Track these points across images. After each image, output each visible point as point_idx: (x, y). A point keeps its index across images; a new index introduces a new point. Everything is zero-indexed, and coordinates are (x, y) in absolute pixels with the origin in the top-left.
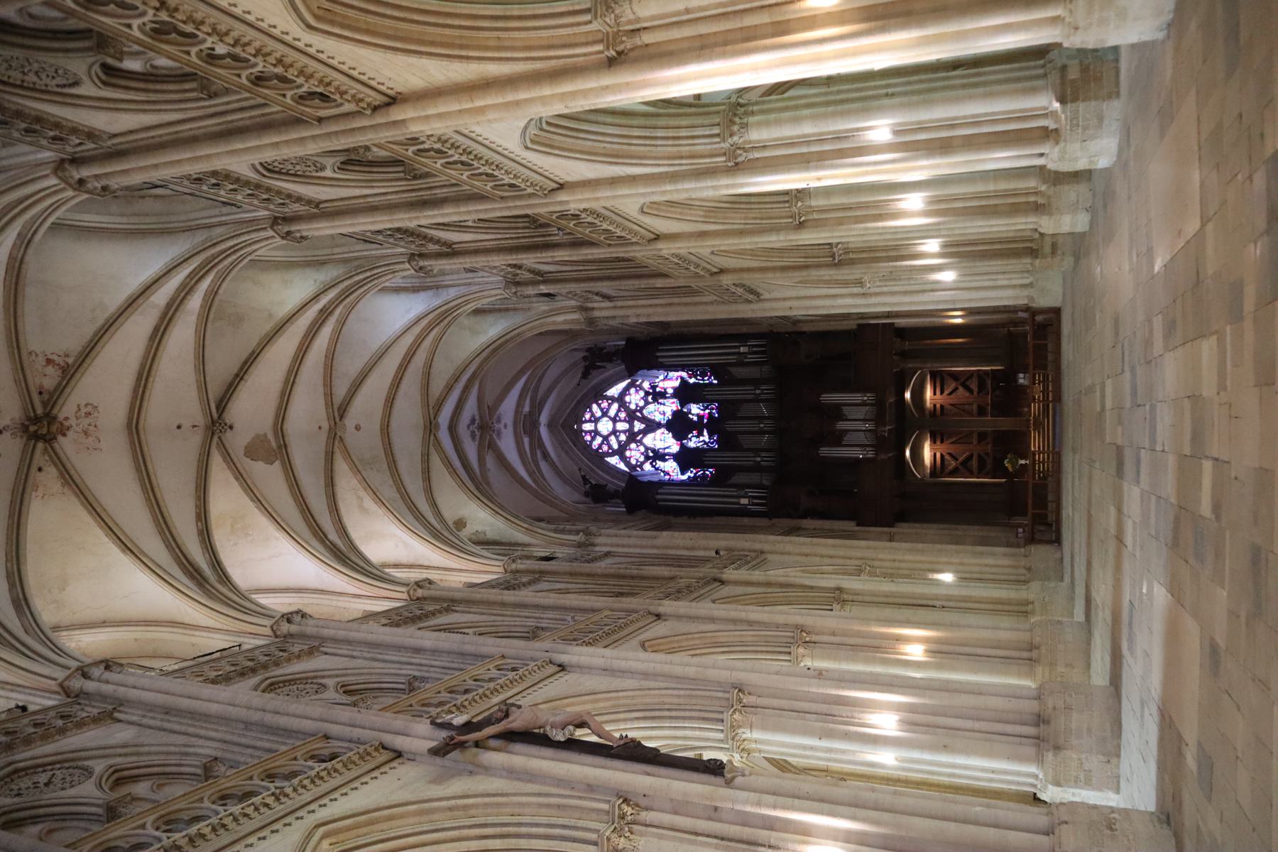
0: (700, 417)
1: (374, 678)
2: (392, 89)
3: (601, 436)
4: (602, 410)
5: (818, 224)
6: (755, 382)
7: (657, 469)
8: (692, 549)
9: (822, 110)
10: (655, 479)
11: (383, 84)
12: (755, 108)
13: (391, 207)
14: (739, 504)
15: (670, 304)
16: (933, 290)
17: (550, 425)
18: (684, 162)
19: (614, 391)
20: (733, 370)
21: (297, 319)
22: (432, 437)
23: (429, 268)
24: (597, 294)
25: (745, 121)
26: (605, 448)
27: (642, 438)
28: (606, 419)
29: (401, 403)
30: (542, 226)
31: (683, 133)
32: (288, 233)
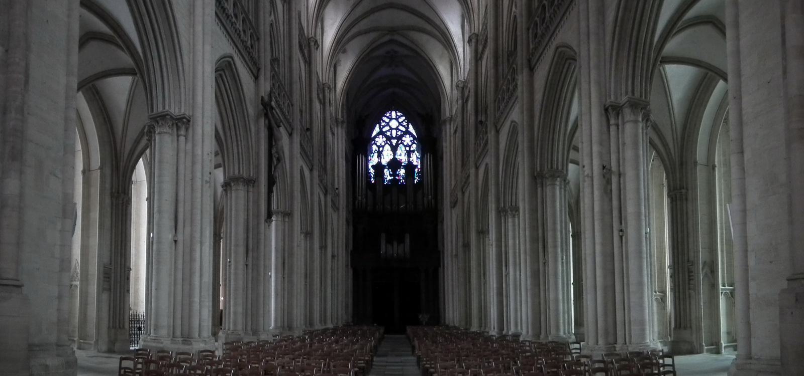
0: (398, 175)
1: (276, 40)
4: (402, 122)
10: (369, 152)
15: (451, 165)
19: (411, 129)
26: (383, 124)
27: (388, 144)
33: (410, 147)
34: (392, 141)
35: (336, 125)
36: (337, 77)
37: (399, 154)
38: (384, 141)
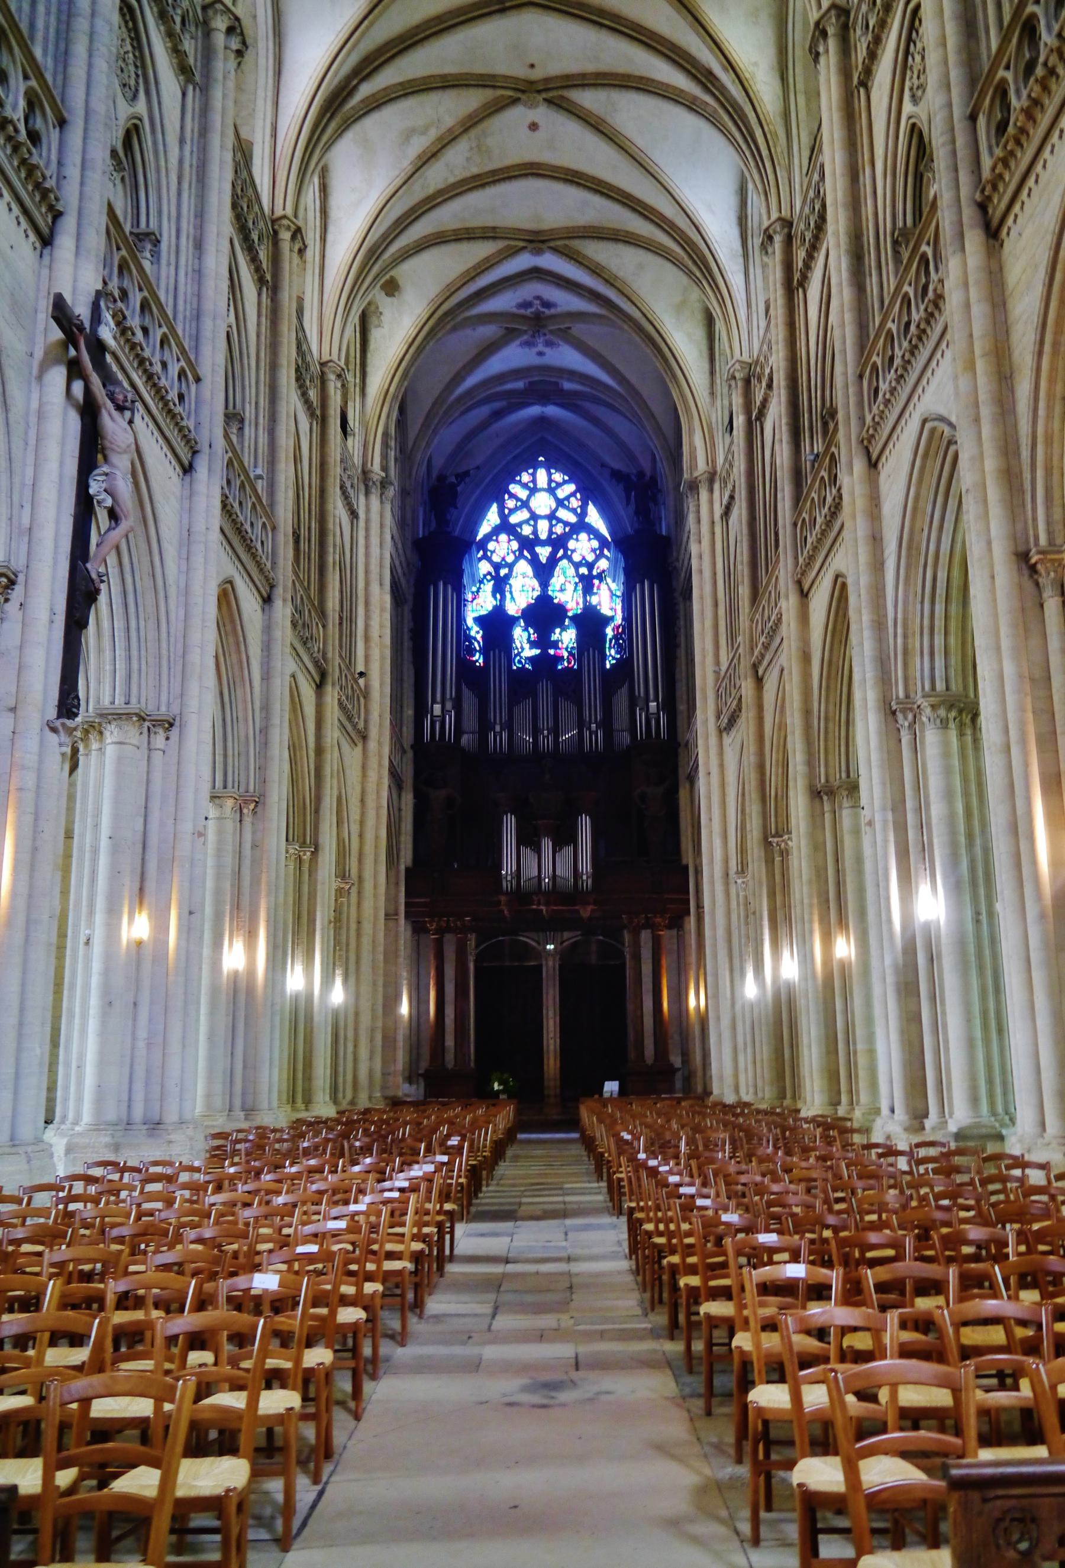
0: (555, 645)
2: (1008, 234)
3: (529, 497)
4: (567, 498)
5: (815, 819)
6: (607, 724)
7: (481, 582)
8: (367, 639)
9: (962, 827)
10: (465, 581)
11: (1015, 221)
12: (969, 739)
13: (855, 204)
14: (434, 702)
15: (716, 605)
16: (731, 970)
17: (542, 421)
18: (900, 641)
19: (594, 517)
20: (624, 691)
21: (698, 34)
22: (521, 244)
23: (770, 250)
24: (732, 497)
25: (952, 725)
27: (526, 558)
28: (554, 506)
29: (573, 194)
30: (825, 424)
31: (939, 640)
32: (824, 34)
33: (590, 566)
34: (538, 549)
35: (362, 488)
36: (369, 355)
37: (558, 588)
38: (514, 552)
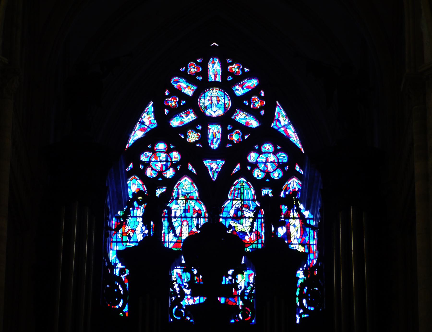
4: (247, 96)
26: (172, 102)
27: (190, 175)
28: (229, 105)
34: (207, 163)
37: (232, 213)
38: (174, 165)
